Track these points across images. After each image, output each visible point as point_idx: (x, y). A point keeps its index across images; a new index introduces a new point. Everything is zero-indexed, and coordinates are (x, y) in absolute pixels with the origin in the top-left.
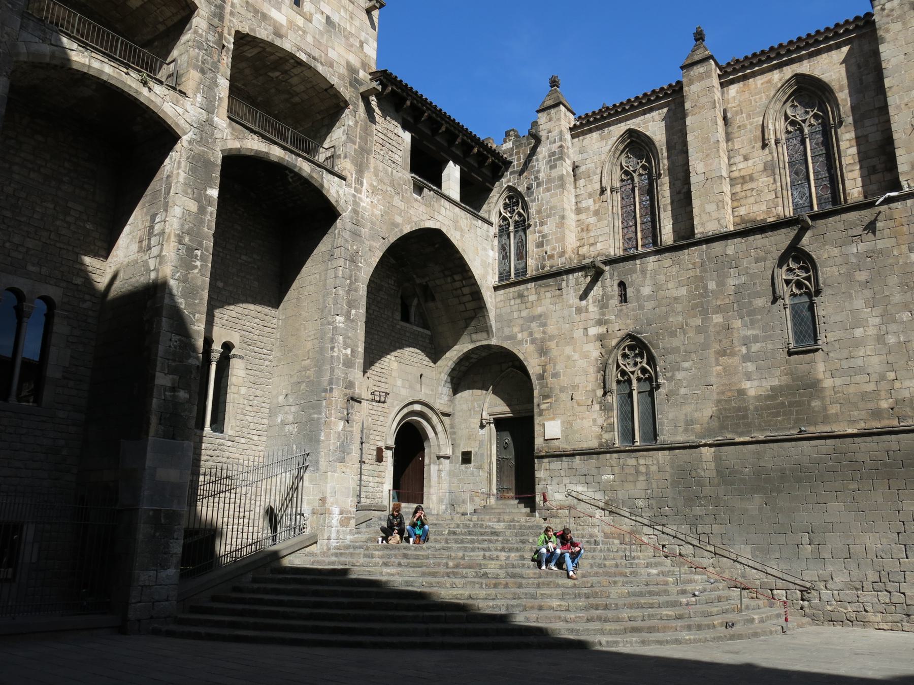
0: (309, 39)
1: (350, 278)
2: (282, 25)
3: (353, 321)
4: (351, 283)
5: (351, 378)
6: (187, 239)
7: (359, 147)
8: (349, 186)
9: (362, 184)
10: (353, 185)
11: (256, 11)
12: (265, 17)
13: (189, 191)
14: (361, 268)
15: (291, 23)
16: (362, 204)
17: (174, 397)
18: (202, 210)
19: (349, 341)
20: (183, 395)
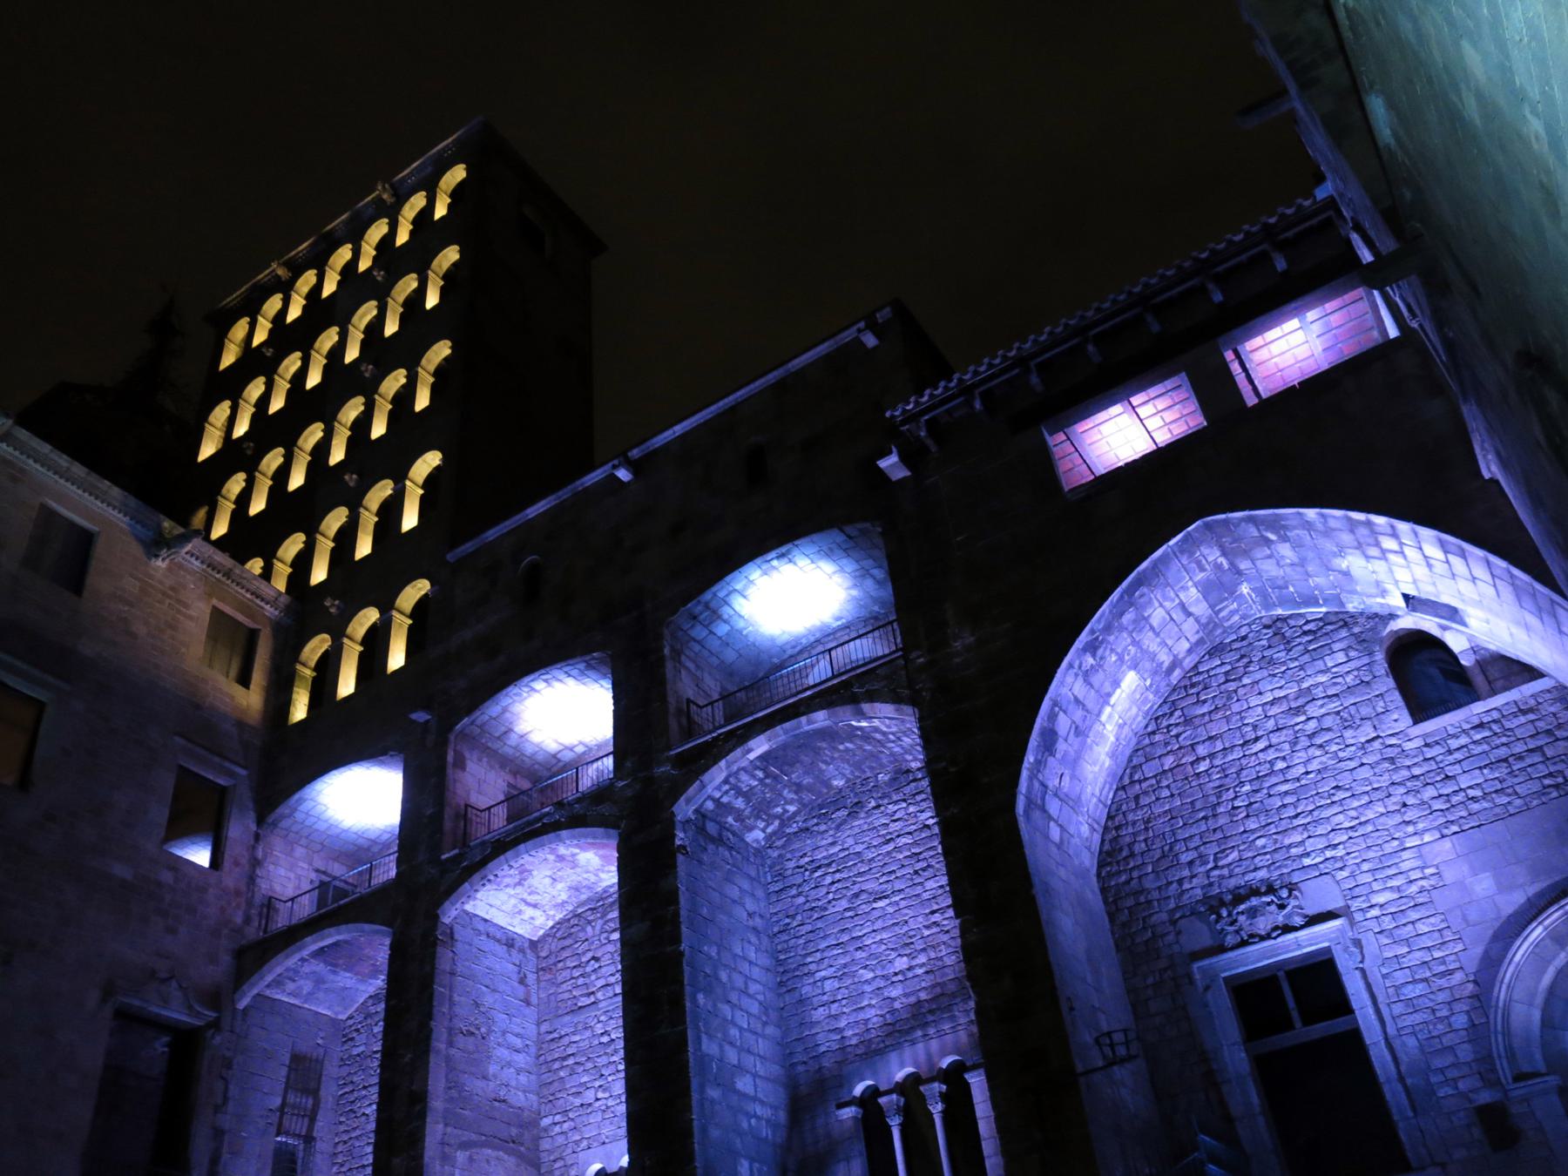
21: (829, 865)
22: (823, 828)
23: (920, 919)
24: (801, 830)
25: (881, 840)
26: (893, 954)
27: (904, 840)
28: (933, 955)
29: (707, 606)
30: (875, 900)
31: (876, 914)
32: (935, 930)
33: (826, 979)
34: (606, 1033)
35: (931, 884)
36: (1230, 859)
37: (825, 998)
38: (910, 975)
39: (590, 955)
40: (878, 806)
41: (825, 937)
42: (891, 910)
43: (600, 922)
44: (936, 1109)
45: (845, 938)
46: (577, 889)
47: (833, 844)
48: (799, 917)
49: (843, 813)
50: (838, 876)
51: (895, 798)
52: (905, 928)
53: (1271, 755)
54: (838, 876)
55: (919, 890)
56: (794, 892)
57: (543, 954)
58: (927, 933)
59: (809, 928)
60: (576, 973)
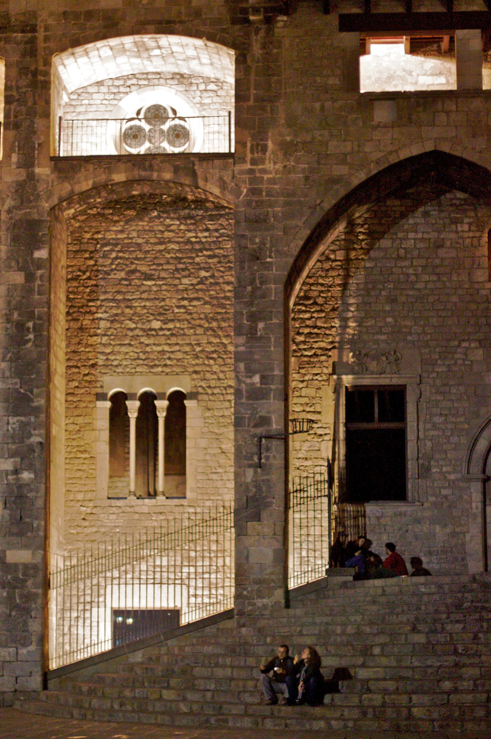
1: (252, 283)
2: (115, 11)
3: (261, 337)
4: (253, 291)
5: (263, 413)
6: (16, 316)
7: (256, 100)
8: (243, 160)
9: (264, 149)
10: (249, 156)
11: (77, 16)
13: (13, 264)
14: (270, 263)
16: (266, 177)
17: (18, 479)
18: (30, 277)
19: (255, 366)
20: (26, 476)
21: (116, 245)
22: (116, 218)
23: (174, 301)
24: (98, 214)
25: (155, 240)
26: (151, 318)
27: (172, 246)
28: (178, 325)
29: (85, 50)
30: (145, 279)
31: (144, 288)
32: (182, 310)
33: (101, 319)
35: (185, 281)
36: (369, 324)
38: (161, 333)
40: (159, 217)
41: (105, 293)
42: (155, 289)
44: (162, 415)
45: (120, 297)
47: (122, 232)
48: (88, 274)
49: (132, 213)
50: (121, 254)
51: (172, 215)
52: (163, 304)
53: (411, 271)
54: (121, 254)
55: (177, 282)
56: (87, 255)
58: (176, 310)
59: (94, 282)
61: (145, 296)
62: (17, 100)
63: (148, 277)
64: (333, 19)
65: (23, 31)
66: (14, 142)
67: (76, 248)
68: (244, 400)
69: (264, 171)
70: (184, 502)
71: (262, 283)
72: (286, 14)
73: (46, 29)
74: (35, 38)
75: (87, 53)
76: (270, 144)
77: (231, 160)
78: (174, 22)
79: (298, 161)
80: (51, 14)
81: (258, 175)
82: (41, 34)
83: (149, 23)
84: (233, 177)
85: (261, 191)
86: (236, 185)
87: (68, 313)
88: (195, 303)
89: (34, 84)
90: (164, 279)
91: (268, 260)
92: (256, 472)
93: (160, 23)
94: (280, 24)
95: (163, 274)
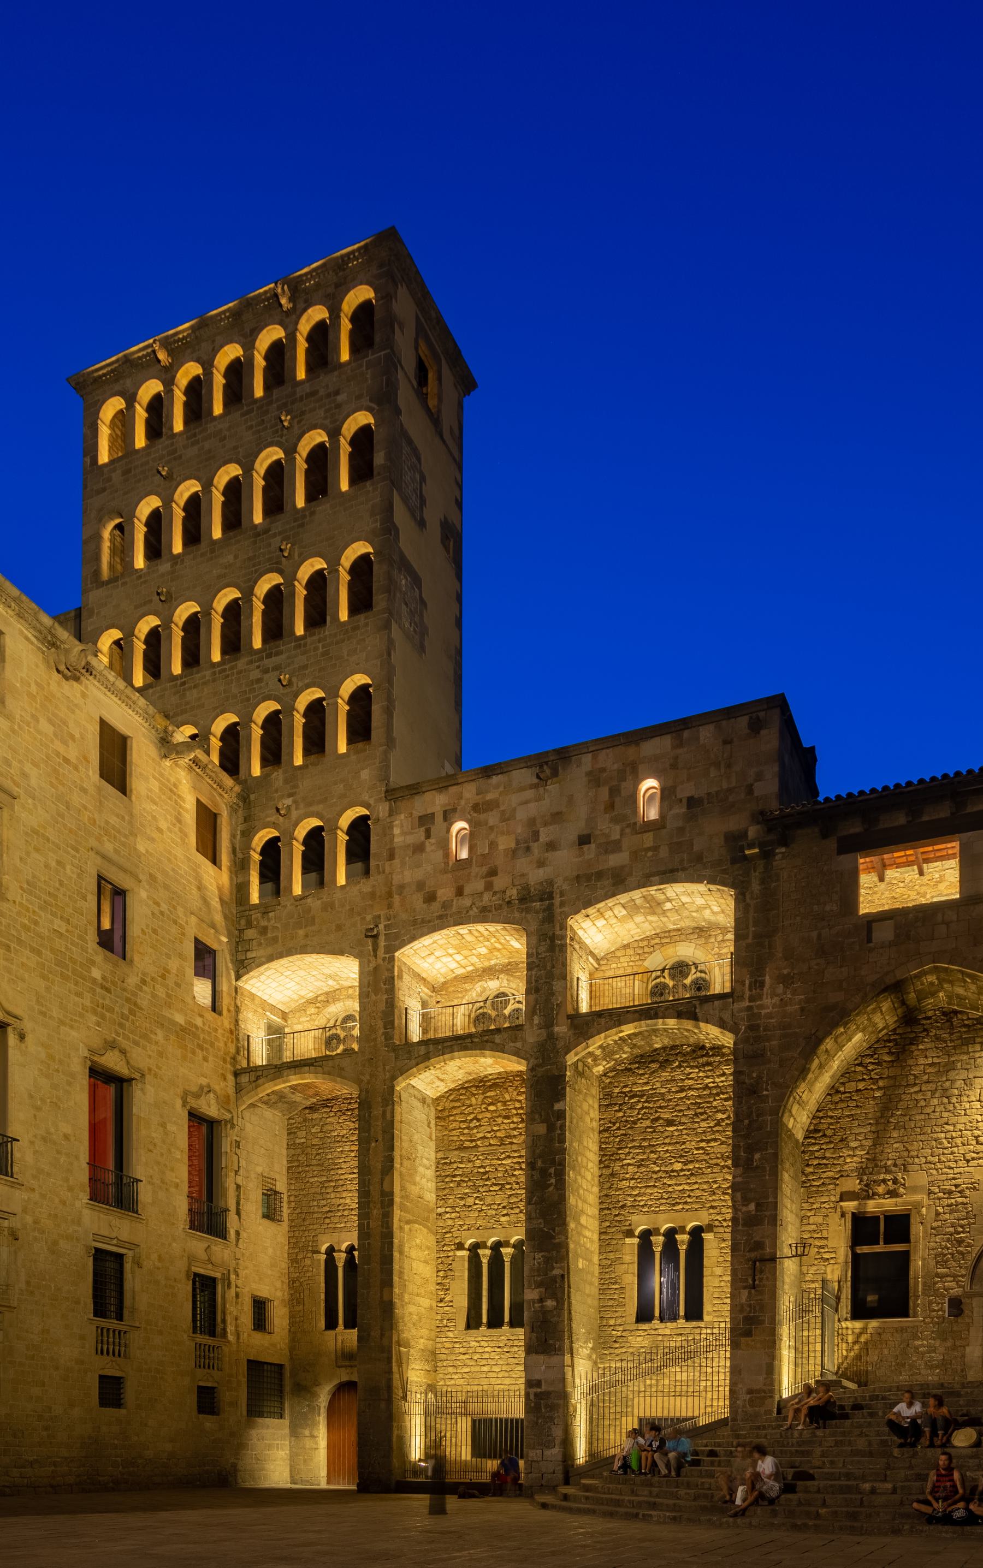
0: (664, 852)
2: (622, 867)
3: (757, 1167)
5: (757, 1239)
8: (741, 998)
9: (762, 985)
10: (747, 993)
11: (588, 878)
12: (600, 875)
14: (767, 1096)
15: (635, 855)
16: (763, 1012)
23: (693, 1143)
26: (674, 1160)
30: (668, 1126)
31: (666, 1134)
33: (629, 1164)
34: (482, 1167)
35: (704, 1124)
37: (627, 1176)
38: (682, 1174)
39: (472, 1116)
41: (633, 1141)
42: (676, 1134)
43: (481, 1097)
45: (645, 1144)
46: (470, 1074)
48: (617, 1125)
52: (683, 1147)
57: (440, 1108)
60: (463, 1126)
61: (667, 1141)
62: (538, 966)
63: (670, 1123)
64: (832, 844)
65: (541, 900)
66: (535, 1006)
67: (607, 1102)
68: (740, 1228)
69: (761, 1007)
70: (702, 1324)
71: (758, 1116)
72: (785, 844)
73: (562, 895)
74: (552, 904)
75: (601, 914)
76: (767, 978)
77: (731, 1000)
78: (677, 870)
79: (794, 993)
80: (565, 879)
81: (756, 1011)
82: (557, 901)
83: (654, 875)
84: (733, 1015)
85: (758, 1026)
86: (735, 1023)
87: (601, 1162)
88: (712, 1144)
89: (552, 948)
90: (684, 1123)
91: (765, 1093)
92: (750, 1293)
93: (664, 873)
94: (778, 857)
95: (683, 1120)
